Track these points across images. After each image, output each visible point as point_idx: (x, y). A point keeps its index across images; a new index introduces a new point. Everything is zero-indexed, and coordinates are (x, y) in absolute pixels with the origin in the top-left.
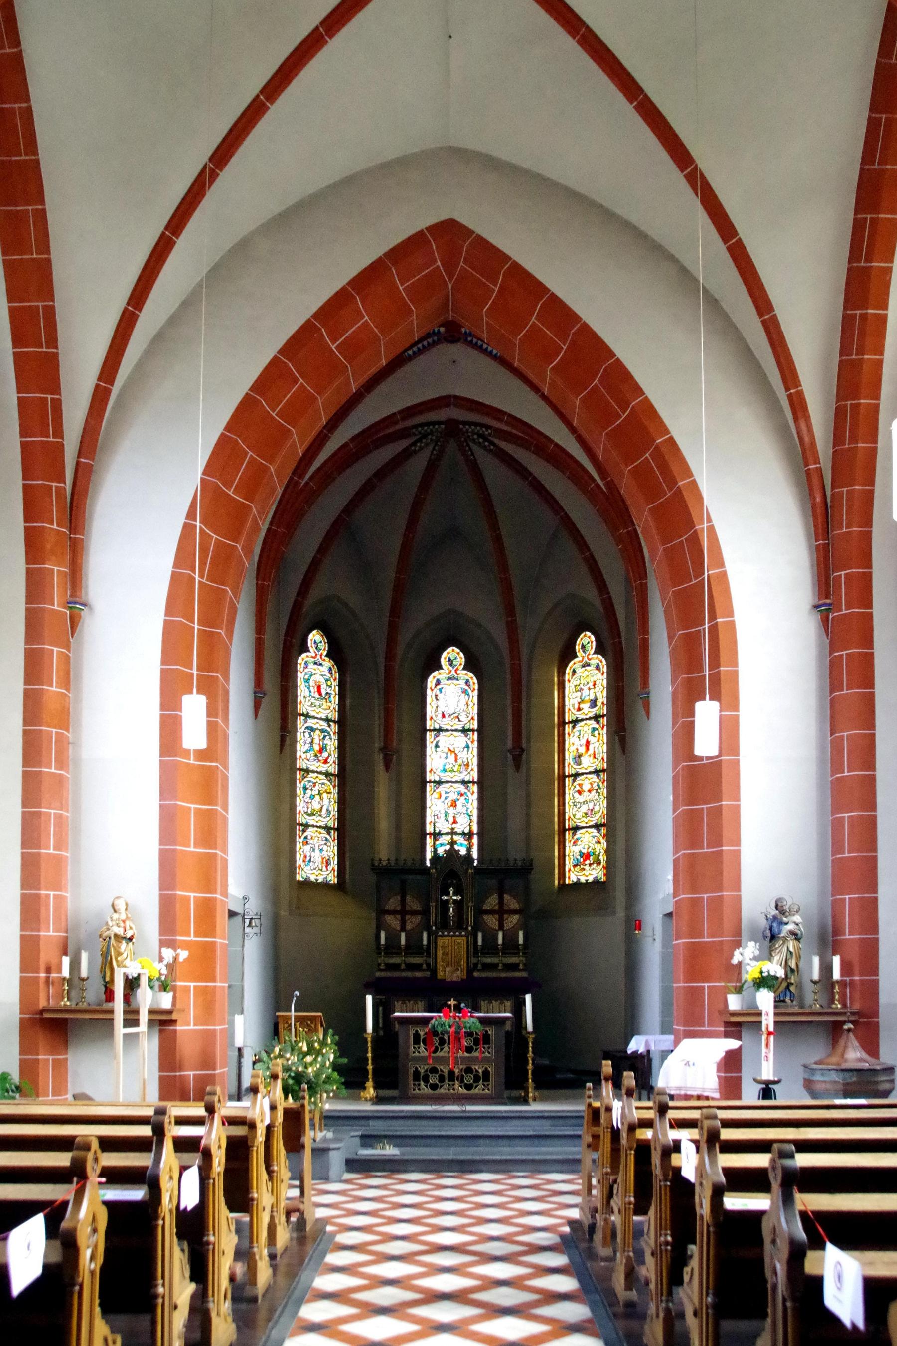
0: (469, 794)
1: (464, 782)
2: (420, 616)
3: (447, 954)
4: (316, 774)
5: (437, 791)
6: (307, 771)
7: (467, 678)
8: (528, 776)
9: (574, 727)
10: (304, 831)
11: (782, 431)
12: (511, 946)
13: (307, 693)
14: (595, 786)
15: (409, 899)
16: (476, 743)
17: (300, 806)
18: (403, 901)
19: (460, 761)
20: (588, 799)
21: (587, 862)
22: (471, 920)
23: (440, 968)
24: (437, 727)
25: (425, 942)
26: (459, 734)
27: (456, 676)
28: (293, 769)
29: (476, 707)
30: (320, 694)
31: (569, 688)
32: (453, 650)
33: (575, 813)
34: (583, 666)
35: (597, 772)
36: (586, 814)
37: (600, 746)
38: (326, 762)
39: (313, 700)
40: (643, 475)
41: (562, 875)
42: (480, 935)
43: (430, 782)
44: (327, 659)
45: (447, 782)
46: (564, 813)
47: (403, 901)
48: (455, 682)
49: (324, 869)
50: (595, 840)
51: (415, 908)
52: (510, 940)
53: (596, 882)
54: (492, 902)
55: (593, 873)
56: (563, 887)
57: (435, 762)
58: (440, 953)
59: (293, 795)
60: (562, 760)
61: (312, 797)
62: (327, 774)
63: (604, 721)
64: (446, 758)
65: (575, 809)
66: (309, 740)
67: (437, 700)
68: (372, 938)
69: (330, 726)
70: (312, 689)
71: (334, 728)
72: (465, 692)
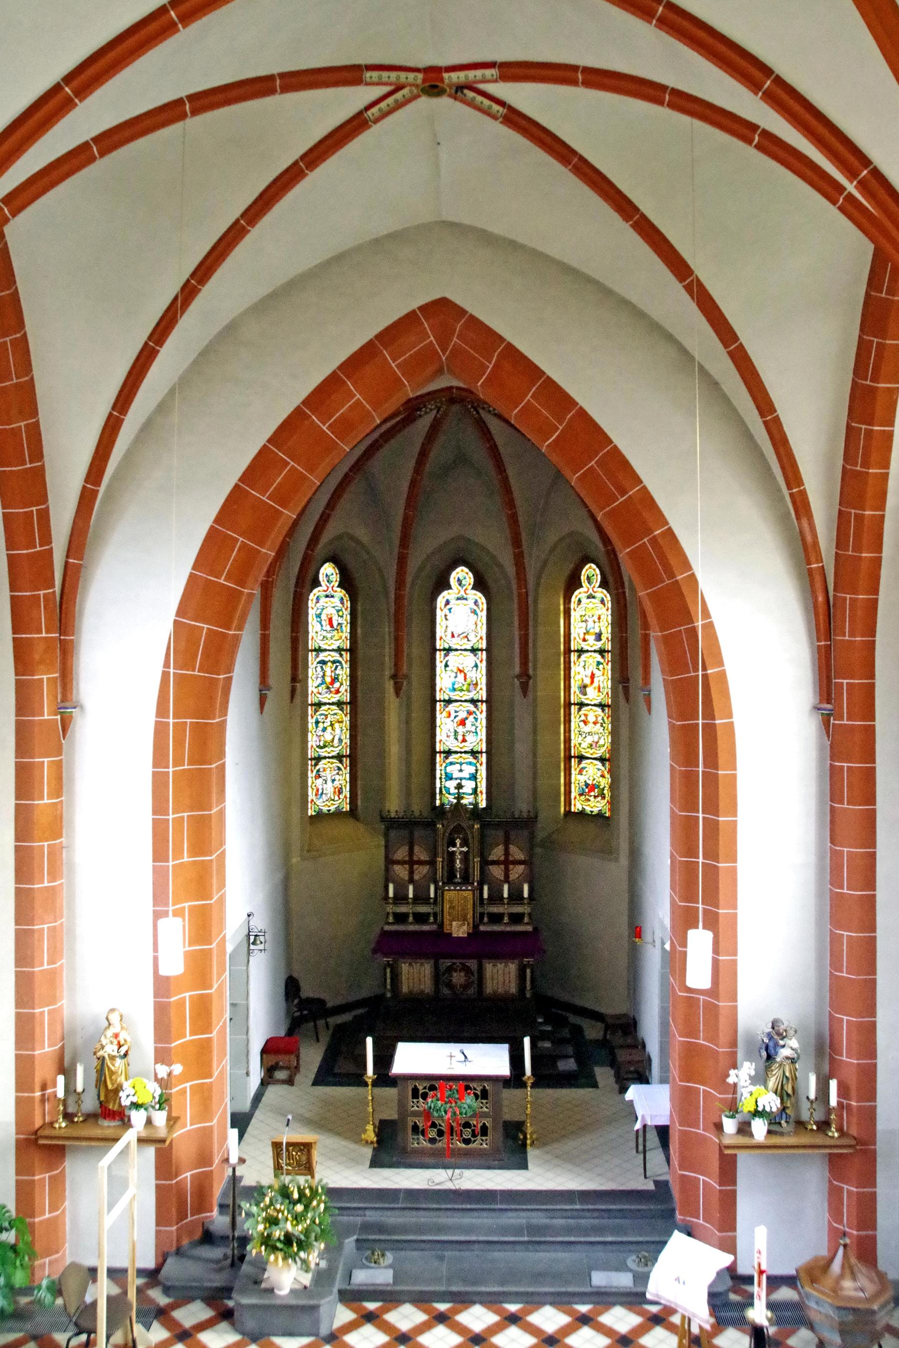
0: (478, 713)
1: (473, 702)
2: (429, 542)
3: (454, 907)
4: (328, 706)
5: (447, 709)
6: (319, 705)
7: (477, 598)
8: (535, 700)
9: (579, 657)
10: (316, 765)
11: (783, 518)
12: (516, 897)
13: (318, 627)
14: (600, 719)
15: (417, 849)
16: (484, 662)
17: (312, 740)
18: (411, 852)
19: (469, 680)
20: (593, 730)
21: (592, 794)
22: (477, 873)
23: (446, 922)
24: (447, 646)
25: (432, 895)
26: (468, 653)
27: (465, 596)
28: (305, 704)
29: (485, 627)
30: (332, 626)
31: (575, 616)
33: (580, 742)
34: (588, 597)
35: (601, 706)
36: (591, 745)
37: (605, 678)
38: (338, 692)
39: (325, 634)
40: (639, 557)
41: (568, 802)
42: (486, 888)
43: (440, 701)
44: (339, 589)
46: (570, 740)
47: (411, 852)
48: (464, 601)
49: (337, 798)
50: (599, 773)
51: (422, 858)
52: (516, 897)
53: (600, 815)
54: (497, 853)
55: (595, 805)
56: (568, 813)
57: (444, 681)
58: (447, 906)
59: (304, 731)
60: (568, 688)
61: (324, 730)
62: (339, 704)
63: (609, 656)
64: (456, 677)
65: (581, 738)
66: (321, 674)
68: (380, 890)
69: (341, 655)
70: (323, 623)
71: (347, 656)
72: (474, 612)
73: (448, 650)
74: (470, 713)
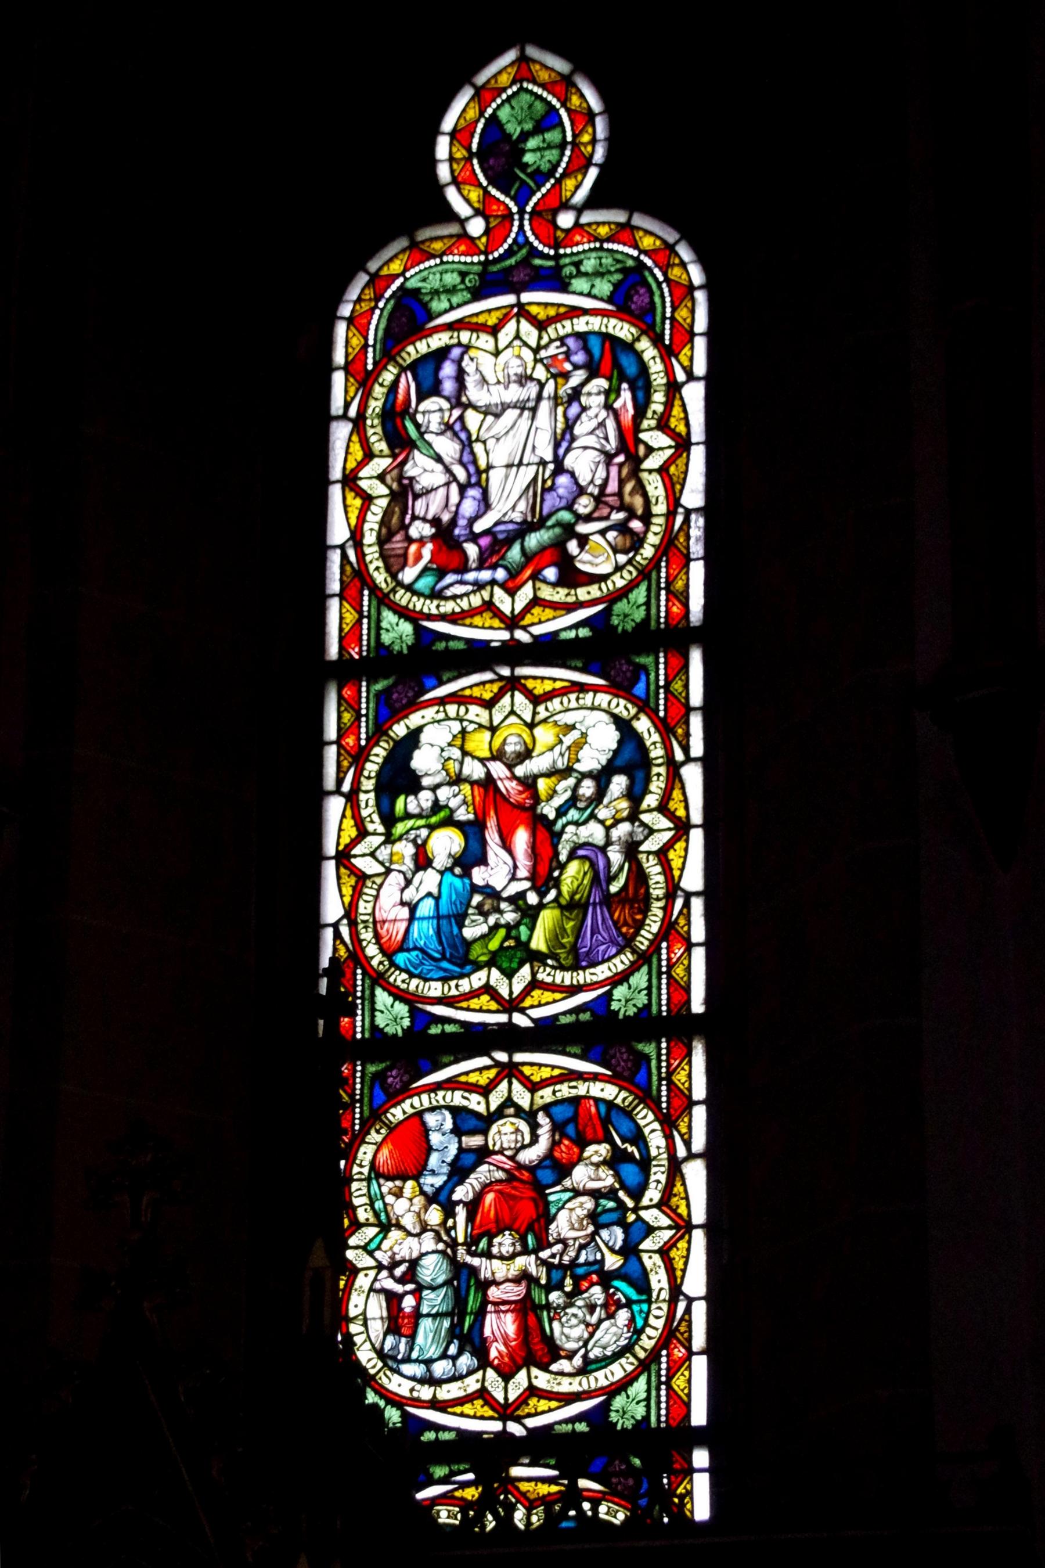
1: (598, 1033)
24: (398, 632)
32: (524, 69)
45: (474, 1040)
57: (381, 887)
67: (401, 443)
72: (609, 360)
74: (577, 1125)
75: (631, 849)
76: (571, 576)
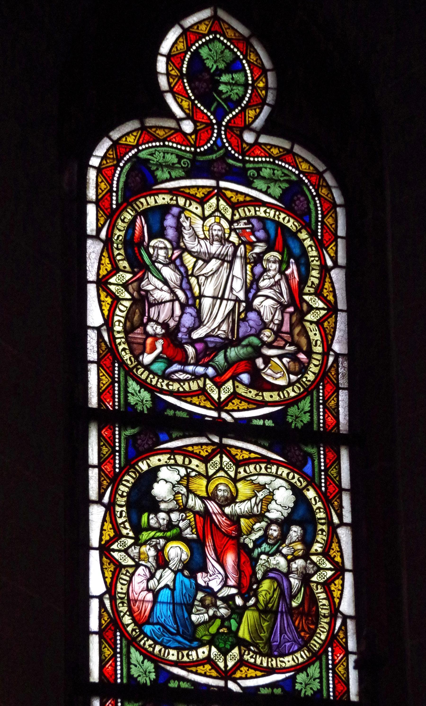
64: (194, 566)
72: (280, 240)
73: (156, 425)
75: (306, 579)
76: (258, 383)
